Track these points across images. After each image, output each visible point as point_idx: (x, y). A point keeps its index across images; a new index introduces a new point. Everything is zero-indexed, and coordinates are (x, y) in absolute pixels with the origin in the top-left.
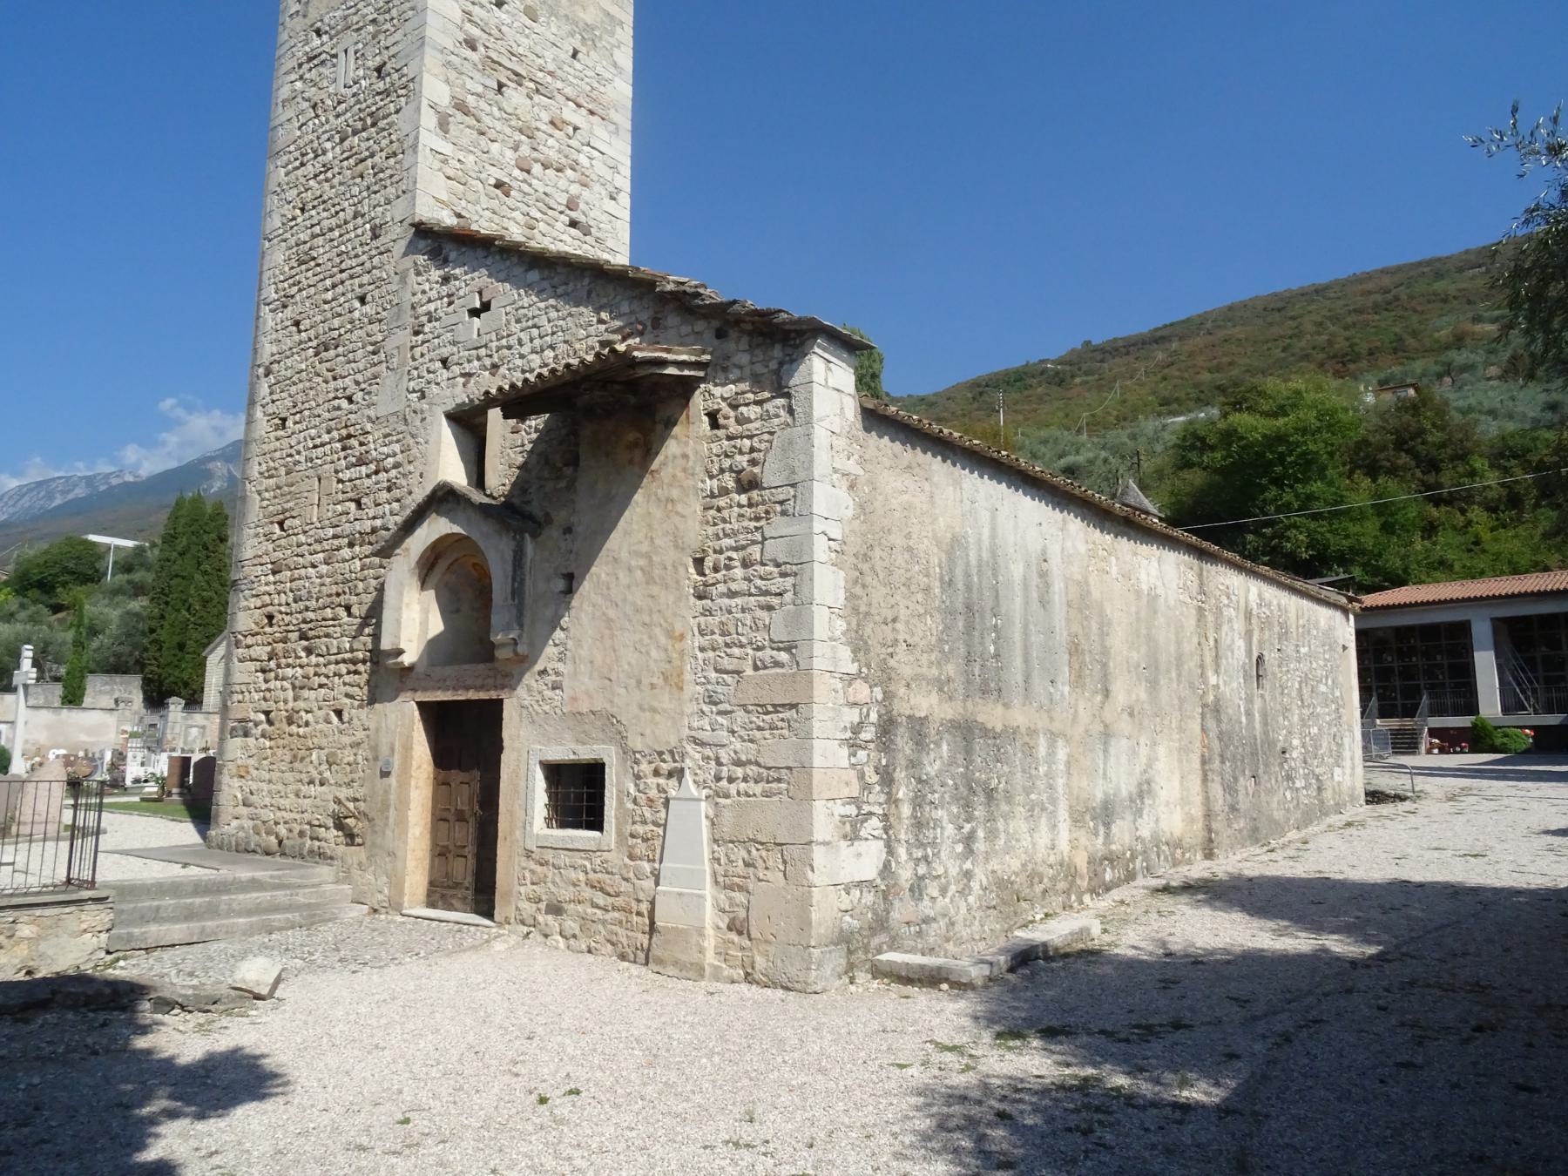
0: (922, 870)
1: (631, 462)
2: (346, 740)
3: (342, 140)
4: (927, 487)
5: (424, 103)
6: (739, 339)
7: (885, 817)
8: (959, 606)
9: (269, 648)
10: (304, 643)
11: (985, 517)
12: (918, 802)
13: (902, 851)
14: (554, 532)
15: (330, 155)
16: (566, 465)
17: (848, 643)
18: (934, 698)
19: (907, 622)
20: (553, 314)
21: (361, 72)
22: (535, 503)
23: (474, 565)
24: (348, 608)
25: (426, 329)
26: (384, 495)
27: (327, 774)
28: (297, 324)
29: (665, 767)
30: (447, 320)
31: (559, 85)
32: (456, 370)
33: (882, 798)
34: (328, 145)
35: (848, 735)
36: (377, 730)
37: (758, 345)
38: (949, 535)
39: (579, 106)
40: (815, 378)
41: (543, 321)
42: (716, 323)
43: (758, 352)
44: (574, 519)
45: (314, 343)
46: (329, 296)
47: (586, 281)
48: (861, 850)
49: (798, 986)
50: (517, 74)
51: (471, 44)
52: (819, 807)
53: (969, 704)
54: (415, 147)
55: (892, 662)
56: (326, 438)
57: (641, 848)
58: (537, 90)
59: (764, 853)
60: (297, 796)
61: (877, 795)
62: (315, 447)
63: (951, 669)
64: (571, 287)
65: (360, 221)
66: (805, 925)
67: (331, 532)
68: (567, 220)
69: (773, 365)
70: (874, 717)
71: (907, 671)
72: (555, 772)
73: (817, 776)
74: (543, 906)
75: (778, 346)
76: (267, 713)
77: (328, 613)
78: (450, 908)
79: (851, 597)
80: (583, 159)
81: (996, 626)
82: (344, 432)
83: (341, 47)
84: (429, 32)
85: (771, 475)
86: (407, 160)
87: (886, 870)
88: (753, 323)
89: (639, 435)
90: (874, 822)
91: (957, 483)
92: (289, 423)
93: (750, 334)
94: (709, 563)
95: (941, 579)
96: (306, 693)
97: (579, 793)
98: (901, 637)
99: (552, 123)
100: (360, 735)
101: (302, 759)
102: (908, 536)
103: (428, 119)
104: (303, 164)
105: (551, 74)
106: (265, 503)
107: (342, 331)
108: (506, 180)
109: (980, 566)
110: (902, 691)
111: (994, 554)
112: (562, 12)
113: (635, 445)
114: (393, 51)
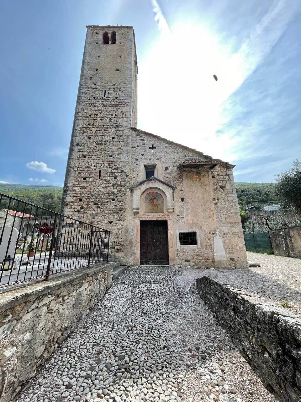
1: (196, 181)
9: (80, 206)
29: (212, 233)
41: (171, 153)
57: (208, 247)
64: (177, 149)
74: (184, 260)
94: (216, 199)
96: (97, 217)
113: (197, 178)
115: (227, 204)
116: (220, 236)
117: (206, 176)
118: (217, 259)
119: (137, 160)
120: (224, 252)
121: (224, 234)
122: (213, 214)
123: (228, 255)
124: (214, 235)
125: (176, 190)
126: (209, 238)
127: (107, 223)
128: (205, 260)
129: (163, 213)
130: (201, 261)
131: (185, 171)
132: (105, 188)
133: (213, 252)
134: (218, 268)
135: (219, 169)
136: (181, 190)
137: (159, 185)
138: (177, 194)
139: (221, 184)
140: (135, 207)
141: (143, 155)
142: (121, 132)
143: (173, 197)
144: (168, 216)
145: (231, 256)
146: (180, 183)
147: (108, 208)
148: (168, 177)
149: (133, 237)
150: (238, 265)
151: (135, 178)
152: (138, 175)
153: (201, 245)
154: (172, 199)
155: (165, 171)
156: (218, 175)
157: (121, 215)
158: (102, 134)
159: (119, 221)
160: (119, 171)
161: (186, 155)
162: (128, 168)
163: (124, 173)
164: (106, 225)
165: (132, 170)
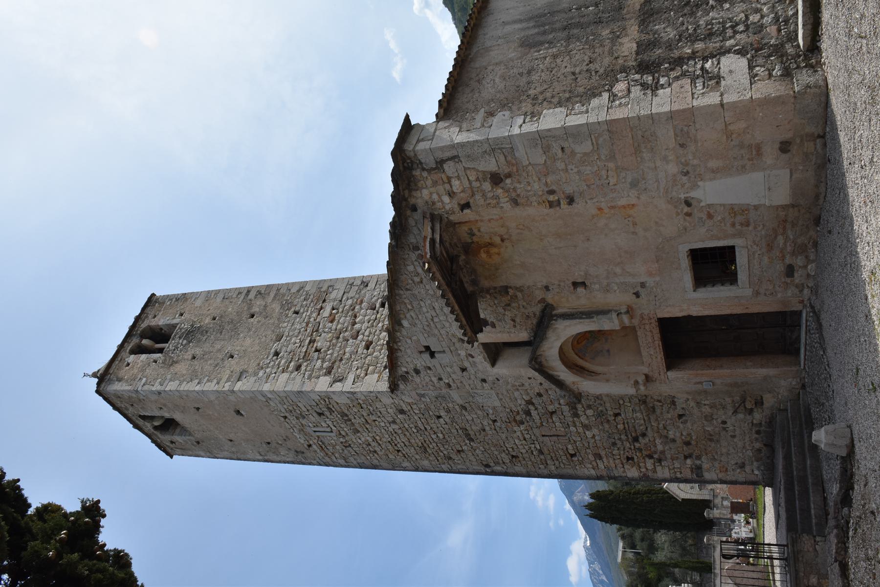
0: (741, 28)
1: (499, 254)
2: (696, 411)
3: (359, 432)
4: (490, 68)
5: (330, 389)
6: (414, 197)
7: (705, 59)
8: (566, 33)
9: (647, 460)
10: (640, 438)
11: (509, 28)
12: (693, 38)
13: (729, 43)
14: (550, 298)
15: (368, 438)
16: (507, 293)
17: (589, 100)
18: (625, 40)
19: (575, 66)
20: (425, 310)
21: (324, 424)
22: (534, 309)
23: (578, 343)
24: (616, 415)
25: (447, 381)
26: (545, 397)
27: (720, 421)
28: (459, 451)
29: (686, 209)
30: (440, 370)
31: (312, 319)
32: (466, 364)
33: (692, 62)
34: (363, 439)
35: (649, 92)
36: (688, 393)
37: (416, 185)
38: (520, 49)
39: (321, 308)
40: (427, 147)
41: (429, 315)
42: (409, 212)
43: (420, 185)
44: (539, 285)
45: (467, 442)
46: (441, 436)
47: (401, 292)
48: (727, 70)
49: (823, 99)
50: (310, 342)
51: (298, 368)
52: (695, 103)
53: (628, 16)
54: (353, 393)
55: (602, 71)
56: (519, 433)
57: (739, 219)
58: (317, 331)
59: (734, 136)
60: (734, 437)
61: (689, 67)
62: (525, 439)
63: (605, 32)
64: (407, 301)
65: (398, 421)
66: (778, 101)
67: (572, 429)
68: (381, 309)
69: (425, 174)
70: (637, 77)
71: (607, 61)
72: (700, 281)
73: (676, 107)
74: (789, 280)
75: (414, 173)
76: (686, 457)
77: (621, 427)
78: (798, 339)
79: (560, 104)
80: (350, 302)
81: (576, 9)
82: (513, 424)
83: (313, 434)
84: (296, 388)
85: (490, 165)
86: (359, 396)
87: (742, 52)
88: (404, 190)
89: (482, 251)
90: (708, 65)
91: (488, 50)
92: (514, 454)
93: (410, 191)
94: (551, 198)
95: (547, 49)
96: (671, 436)
97: (712, 265)
98: (585, 68)
99: (332, 322)
100: (692, 404)
101: (711, 435)
102: (521, 74)
103: (338, 387)
104: (375, 452)
105: (307, 325)
106: (562, 465)
107: (457, 427)
108: (364, 343)
109: (539, 26)
110: (620, 61)
111: (530, 19)
112: (276, 322)
114: (309, 408)
115: (560, 165)
116: (695, 186)
117: (471, 229)
118: (782, 196)
120: (758, 176)
121: (686, 174)
122: (612, 207)
123: (769, 160)
124: (694, 203)
126: (705, 217)
127: (685, 422)
128: (788, 226)
130: (791, 237)
131: (474, 282)
132: (586, 427)
133: (756, 208)
134: (817, 197)
135: (425, 192)
139: (487, 186)
141: (463, 370)
142: (414, 407)
145: (770, 154)
146: (521, 291)
147: (642, 422)
148: (514, 321)
149: (718, 381)
150: (811, 129)
152: (530, 378)
153: (734, 236)
155: (494, 326)
156: (451, 194)
157: (659, 401)
158: (441, 436)
159: (675, 405)
160: (531, 407)
161: (417, 279)
164: (689, 424)
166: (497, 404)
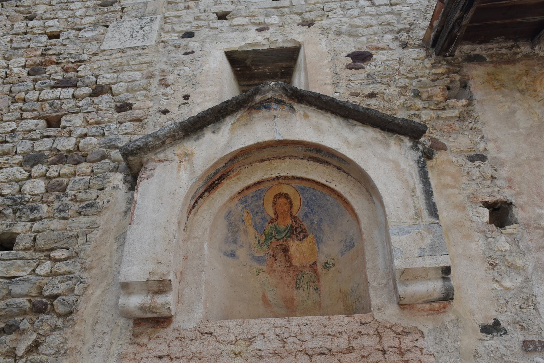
119: (189, 35)
125: (440, 156)
129: (366, 318)
136: (472, 159)
137: (317, 129)
138: (448, 180)
140: (135, 271)
141: (222, 16)
143: (428, 193)
144: (407, 341)
146: (460, 118)
151: (165, 112)
152: (186, 97)
154: (422, 204)
157: (35, 347)
160: (84, 91)
162: (138, 75)
163: (106, 97)
165: (155, 82)
166: (105, 46)
